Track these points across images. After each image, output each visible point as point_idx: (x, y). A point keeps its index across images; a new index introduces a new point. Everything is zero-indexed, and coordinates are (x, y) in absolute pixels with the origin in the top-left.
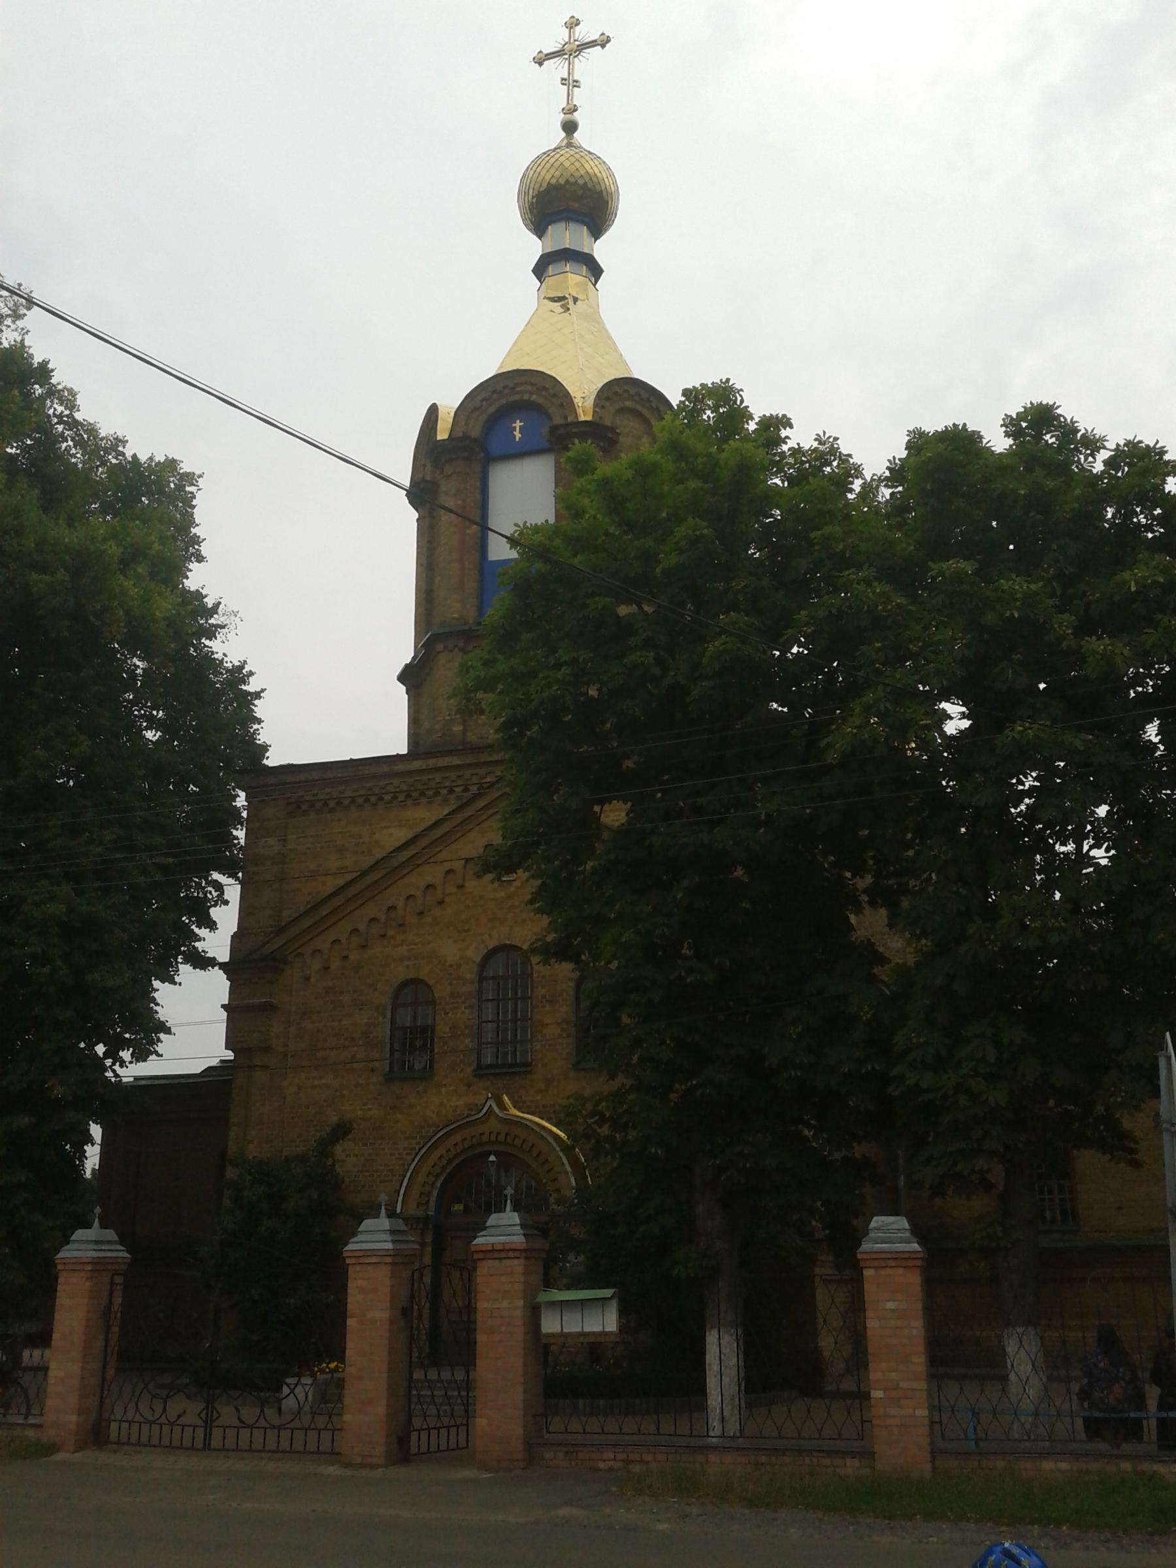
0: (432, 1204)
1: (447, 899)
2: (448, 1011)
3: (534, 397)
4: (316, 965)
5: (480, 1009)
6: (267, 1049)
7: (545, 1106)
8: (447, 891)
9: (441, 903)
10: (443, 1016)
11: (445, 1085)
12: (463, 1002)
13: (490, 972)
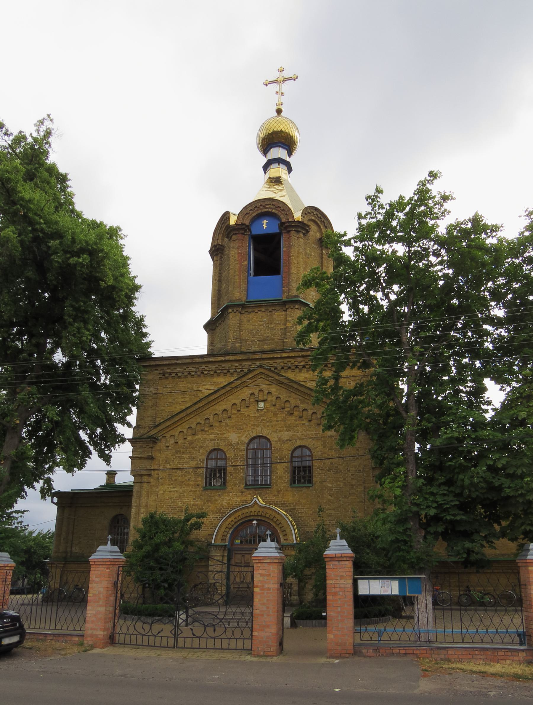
0: (227, 540)
1: (232, 416)
3: (274, 210)
4: (172, 441)
6: (150, 475)
7: (277, 502)
9: (230, 417)
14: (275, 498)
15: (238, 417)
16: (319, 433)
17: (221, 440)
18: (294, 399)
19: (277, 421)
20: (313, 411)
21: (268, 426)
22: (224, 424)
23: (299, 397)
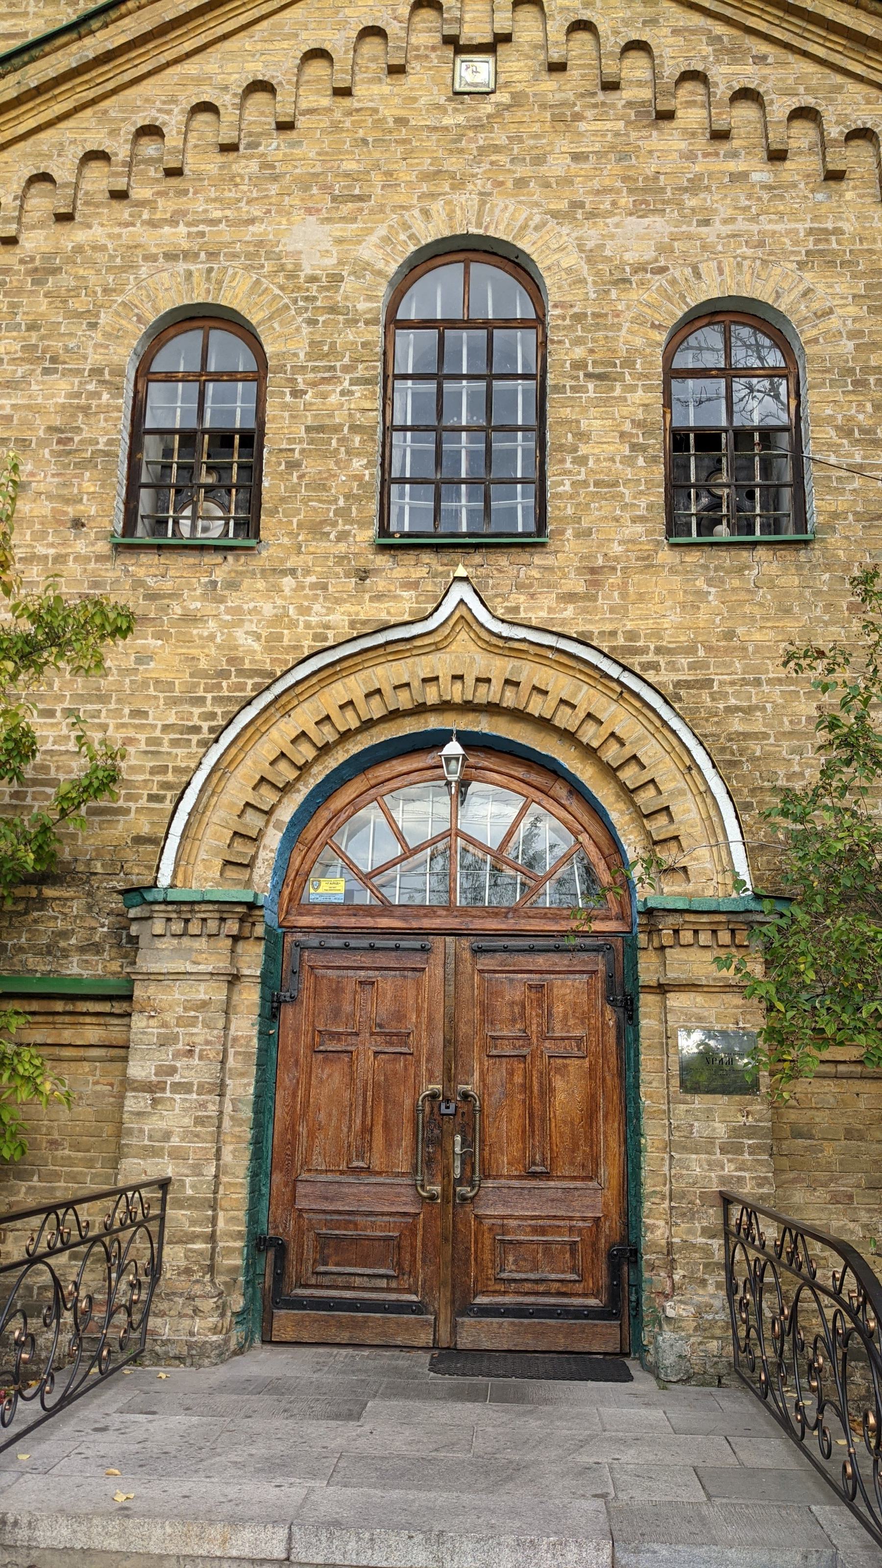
1: (302, 122)
2: (301, 386)
5: (387, 399)
8: (304, 105)
9: (285, 126)
10: (288, 398)
11: (293, 572)
12: (346, 369)
13: (410, 310)
14: (570, 611)
15: (336, 127)
16: (838, 231)
17: (235, 256)
18: (675, 32)
19: (577, 157)
20: (795, 103)
21: (521, 183)
22: (254, 166)
23: (709, 23)
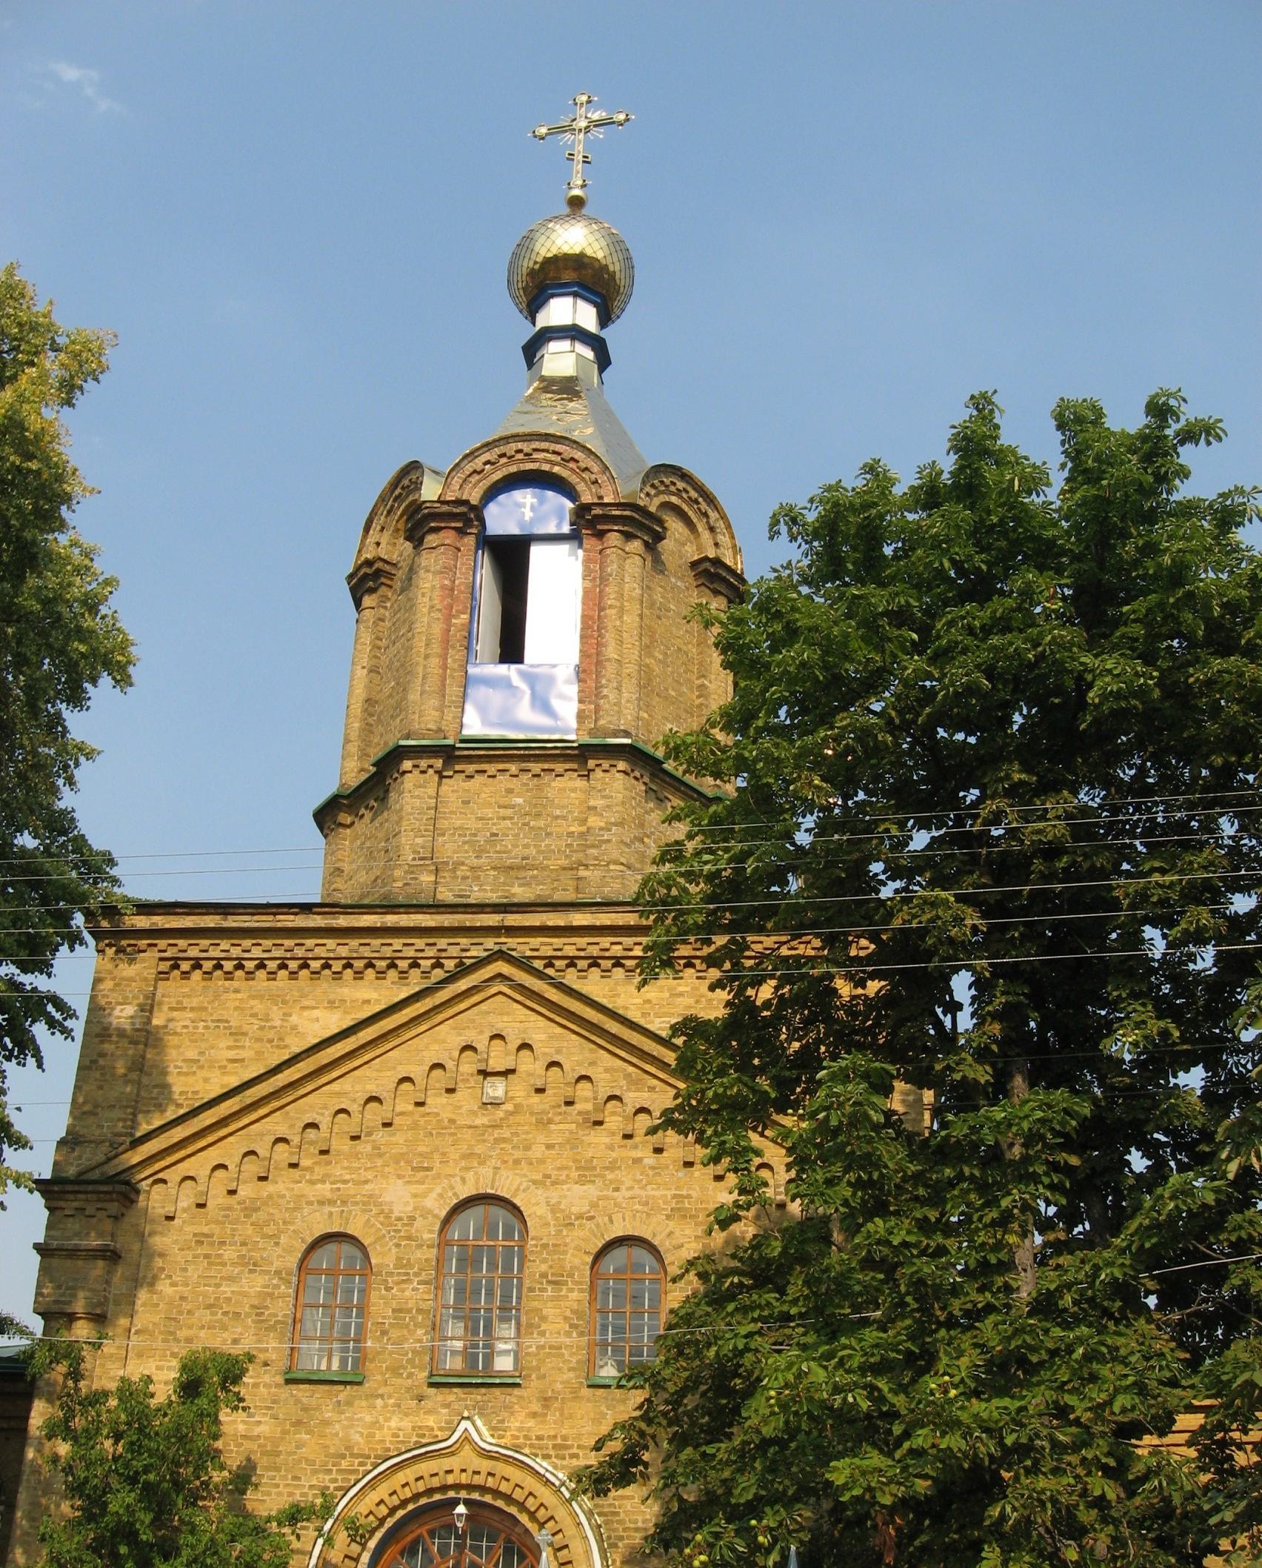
1: (397, 1121)
16: (689, 1197)
17: (357, 1203)
18: (607, 1070)
19: (549, 1147)
21: (517, 1162)
22: (369, 1148)
